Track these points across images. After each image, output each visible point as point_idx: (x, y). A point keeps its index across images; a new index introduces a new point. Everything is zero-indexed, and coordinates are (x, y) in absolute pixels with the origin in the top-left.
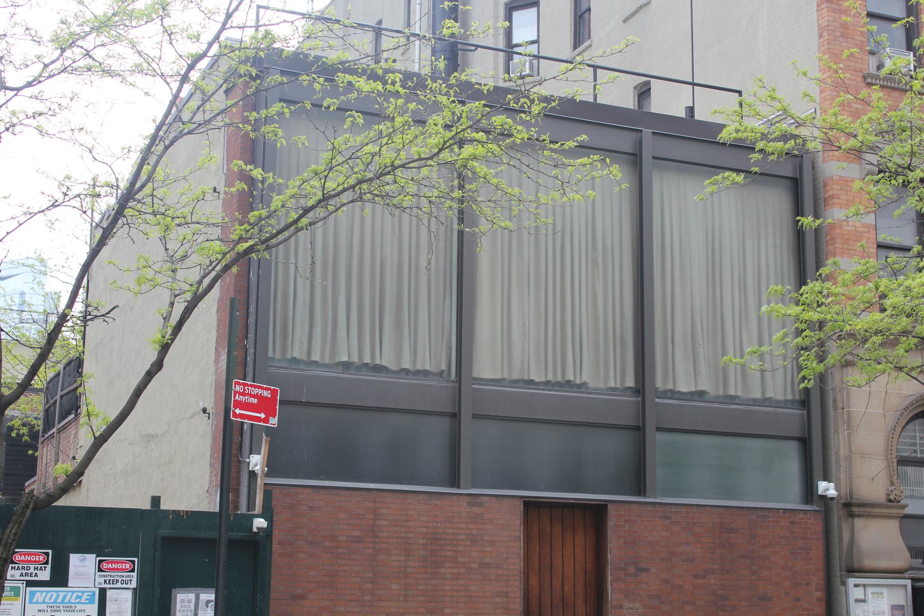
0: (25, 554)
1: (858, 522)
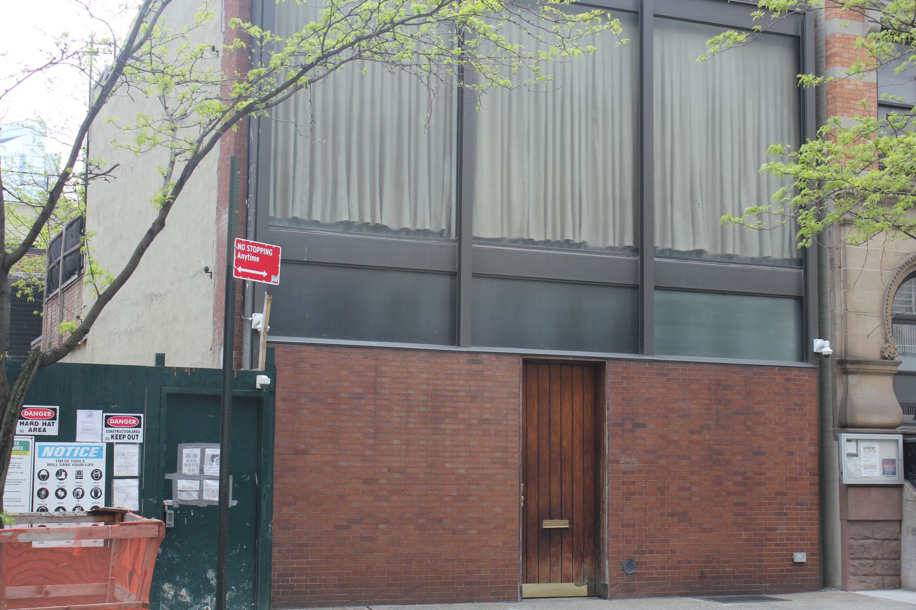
0: (33, 410)
1: (853, 379)
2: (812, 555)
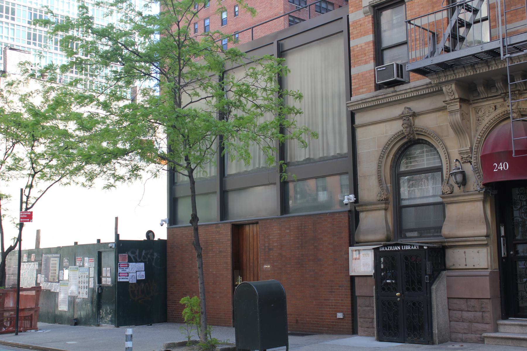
2: (347, 314)
